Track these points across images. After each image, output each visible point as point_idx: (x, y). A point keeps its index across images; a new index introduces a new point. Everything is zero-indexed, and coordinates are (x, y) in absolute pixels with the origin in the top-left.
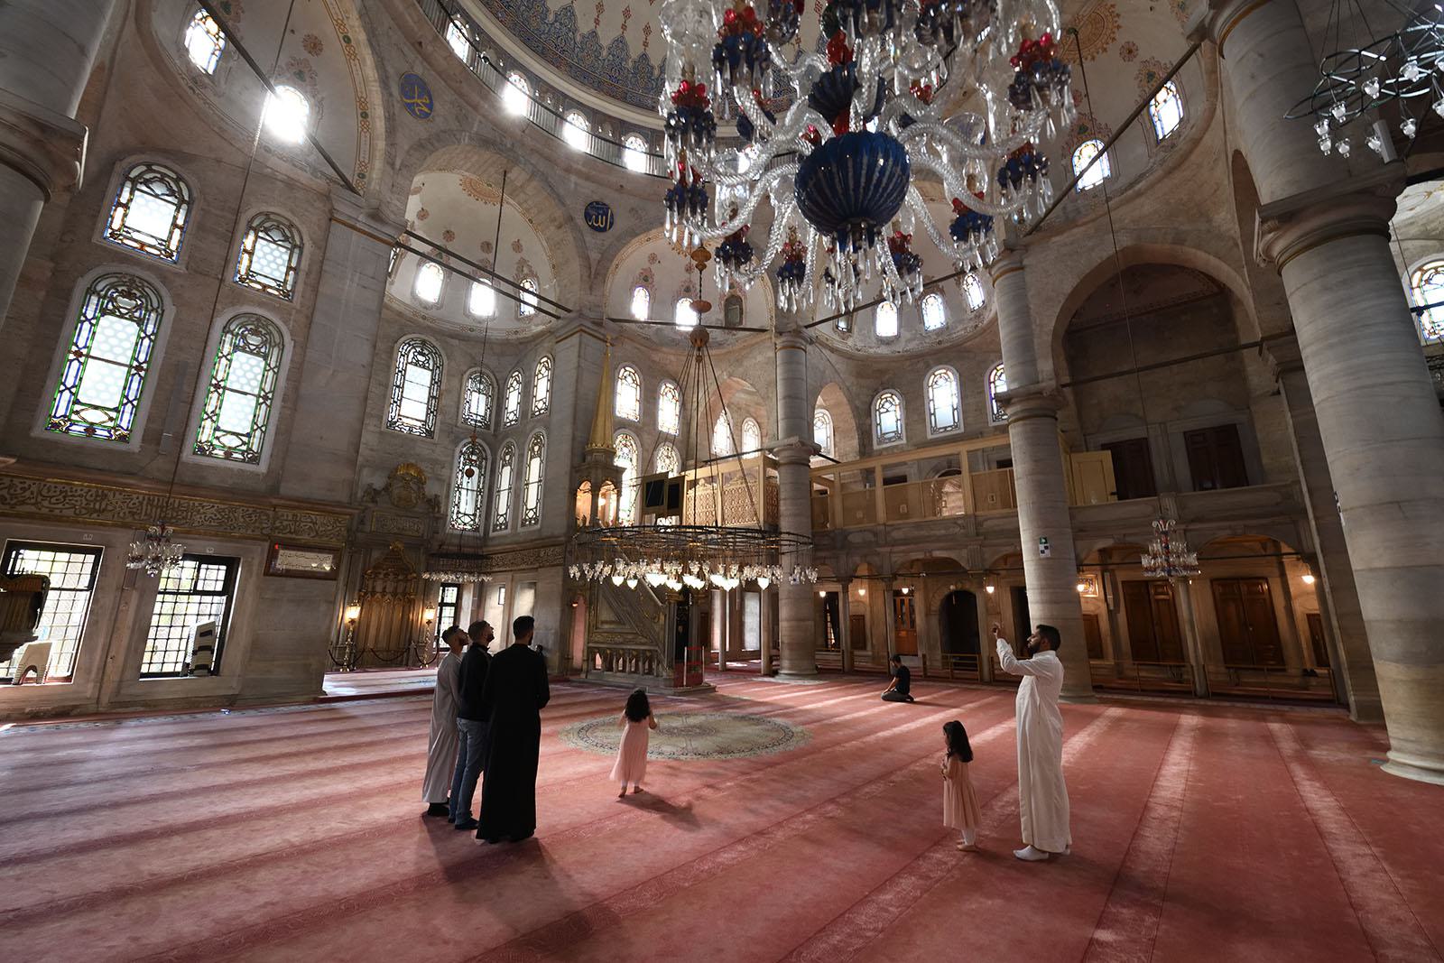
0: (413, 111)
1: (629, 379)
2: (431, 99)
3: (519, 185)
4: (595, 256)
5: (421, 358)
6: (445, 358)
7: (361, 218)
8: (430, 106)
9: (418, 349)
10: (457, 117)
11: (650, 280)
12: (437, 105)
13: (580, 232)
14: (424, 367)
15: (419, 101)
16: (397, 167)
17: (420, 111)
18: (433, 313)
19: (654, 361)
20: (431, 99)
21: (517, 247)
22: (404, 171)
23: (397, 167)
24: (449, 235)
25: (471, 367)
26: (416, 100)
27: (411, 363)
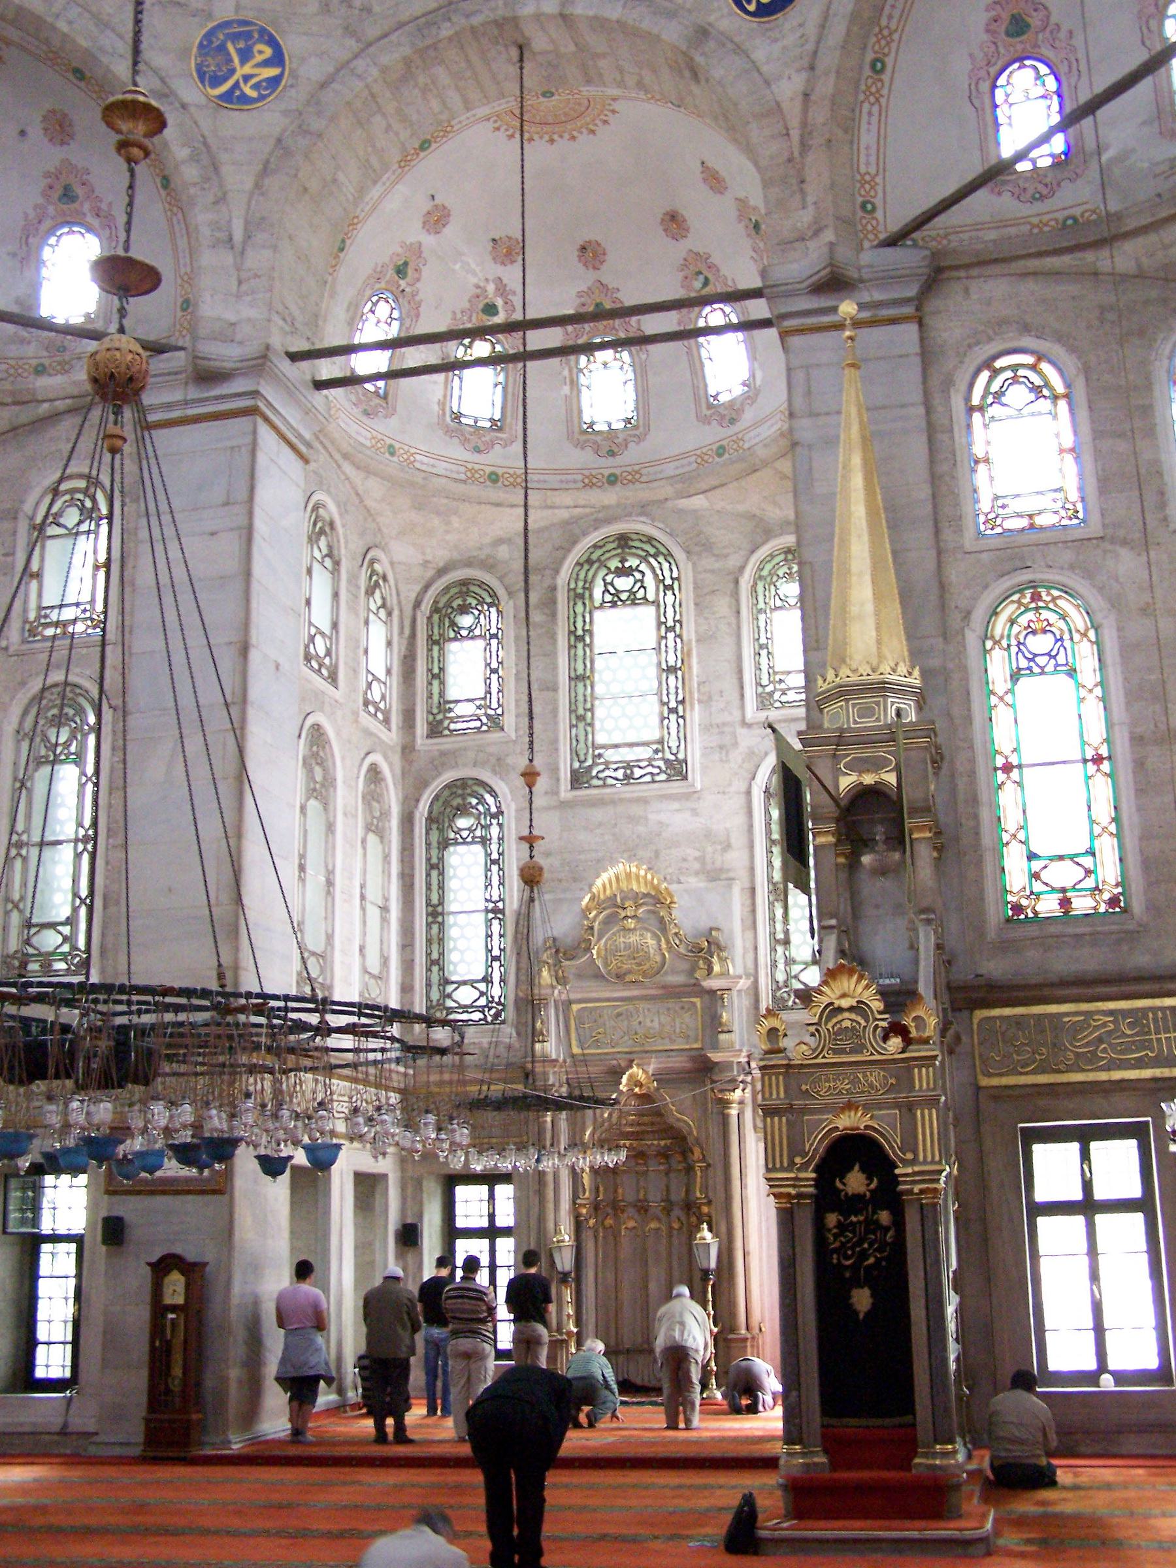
0: (245, 99)
1: (1018, 395)
2: (272, 42)
3: (572, 48)
4: (788, 88)
5: (623, 583)
6: (679, 555)
7: (194, 393)
8: (277, 59)
9: (614, 564)
10: (346, 28)
11: (1035, 20)
12: (291, 44)
13: (739, 50)
14: (633, 601)
15: (247, 69)
16: (238, 236)
17: (256, 87)
18: (632, 455)
19: (1120, 279)
20: (272, 42)
21: (714, 180)
22: (260, 237)
23: (238, 236)
24: (590, 253)
25: (753, 552)
26: (240, 72)
27: (601, 607)
